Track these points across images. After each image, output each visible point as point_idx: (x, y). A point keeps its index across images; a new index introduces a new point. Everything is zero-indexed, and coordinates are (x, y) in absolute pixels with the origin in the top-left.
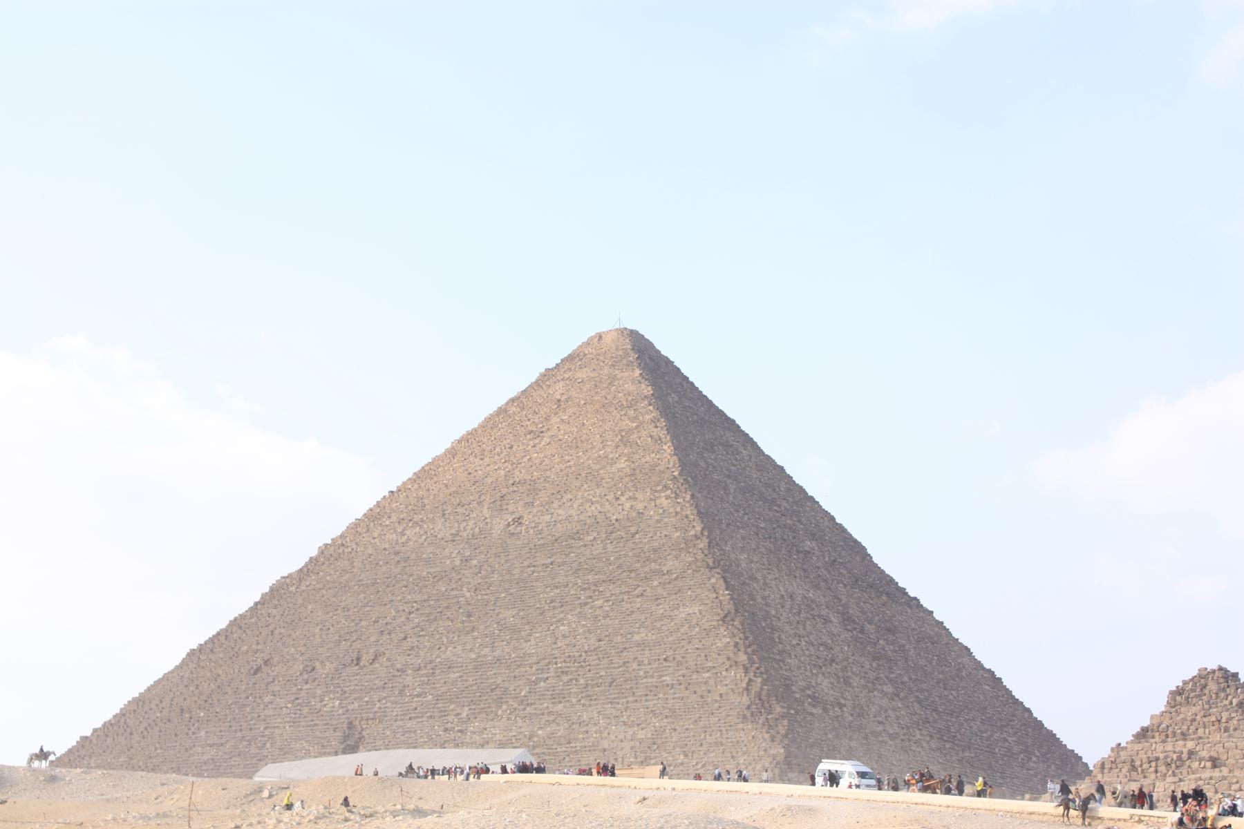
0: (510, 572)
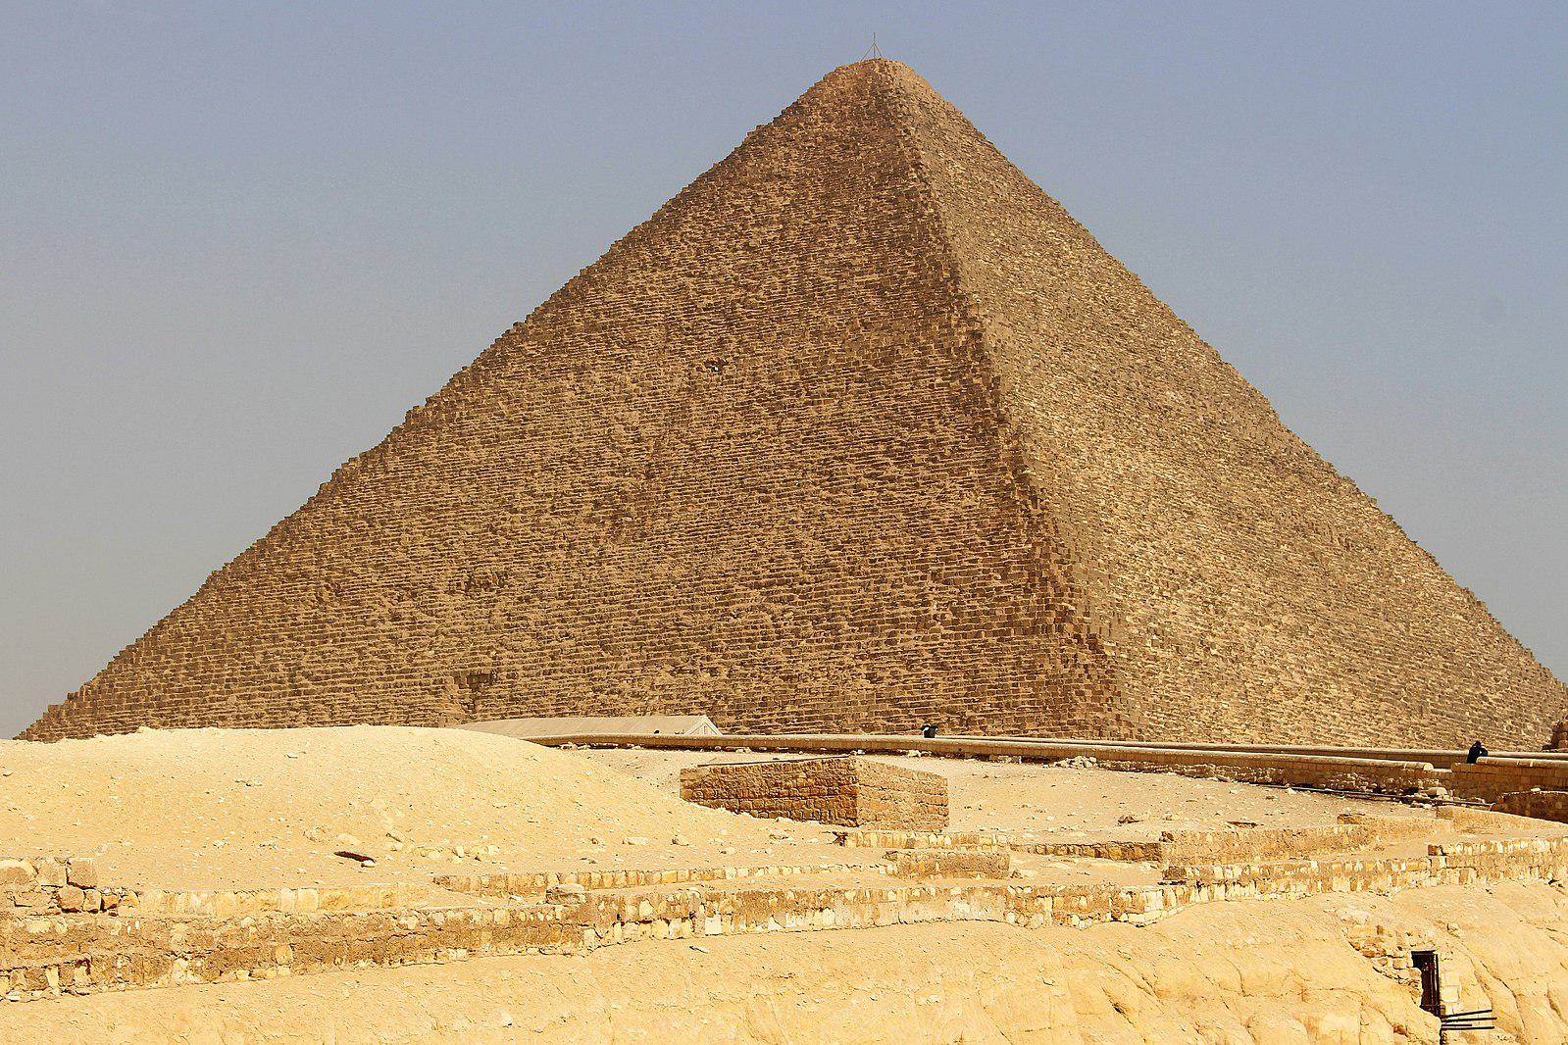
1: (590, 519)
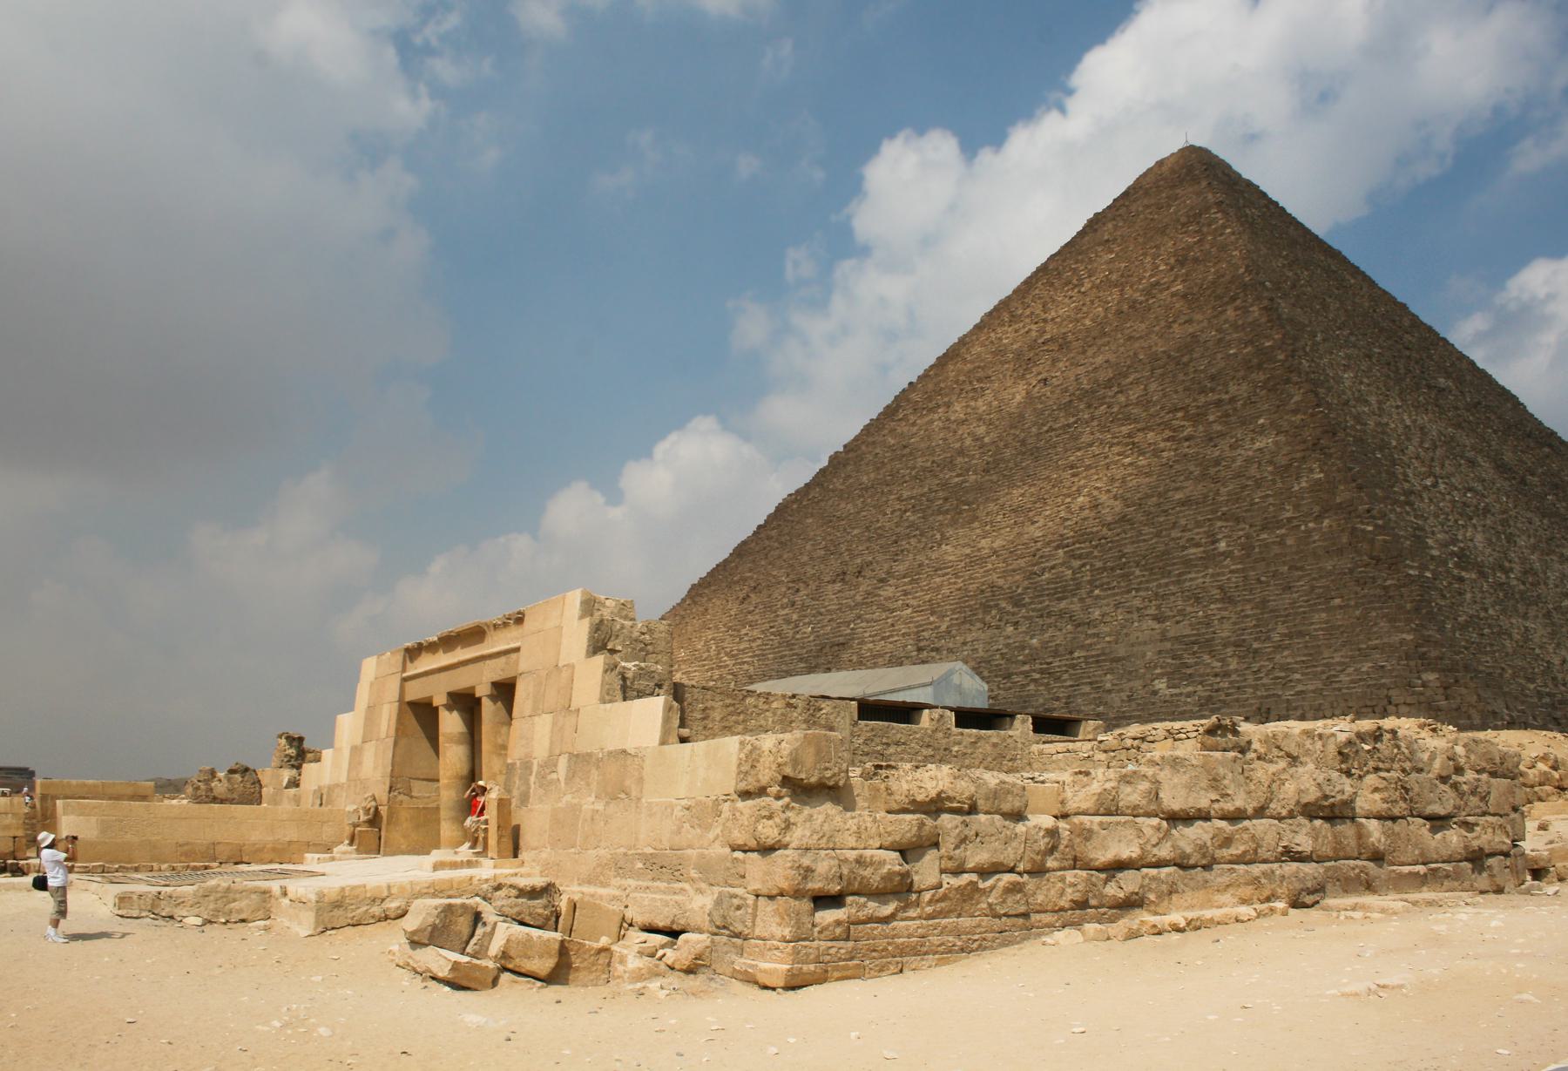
0: (1023, 443)
1: (940, 512)
